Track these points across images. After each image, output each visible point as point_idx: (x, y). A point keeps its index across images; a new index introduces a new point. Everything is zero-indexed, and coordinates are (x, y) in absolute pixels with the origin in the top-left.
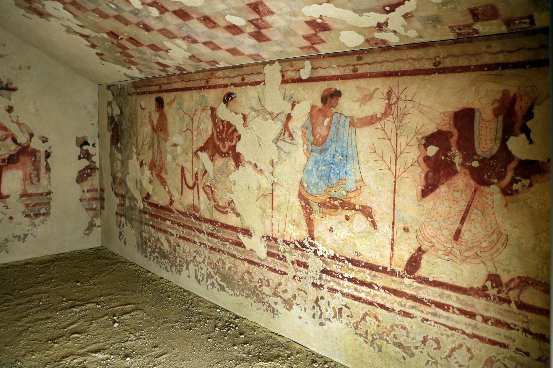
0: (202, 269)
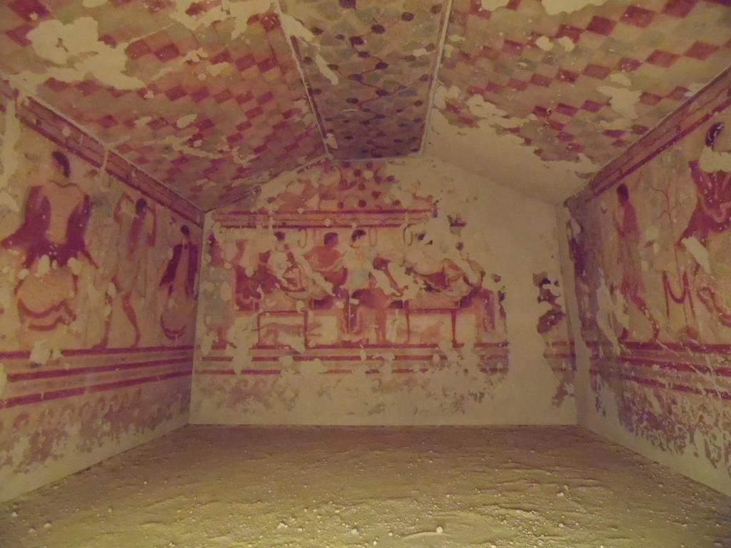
0: (715, 438)
